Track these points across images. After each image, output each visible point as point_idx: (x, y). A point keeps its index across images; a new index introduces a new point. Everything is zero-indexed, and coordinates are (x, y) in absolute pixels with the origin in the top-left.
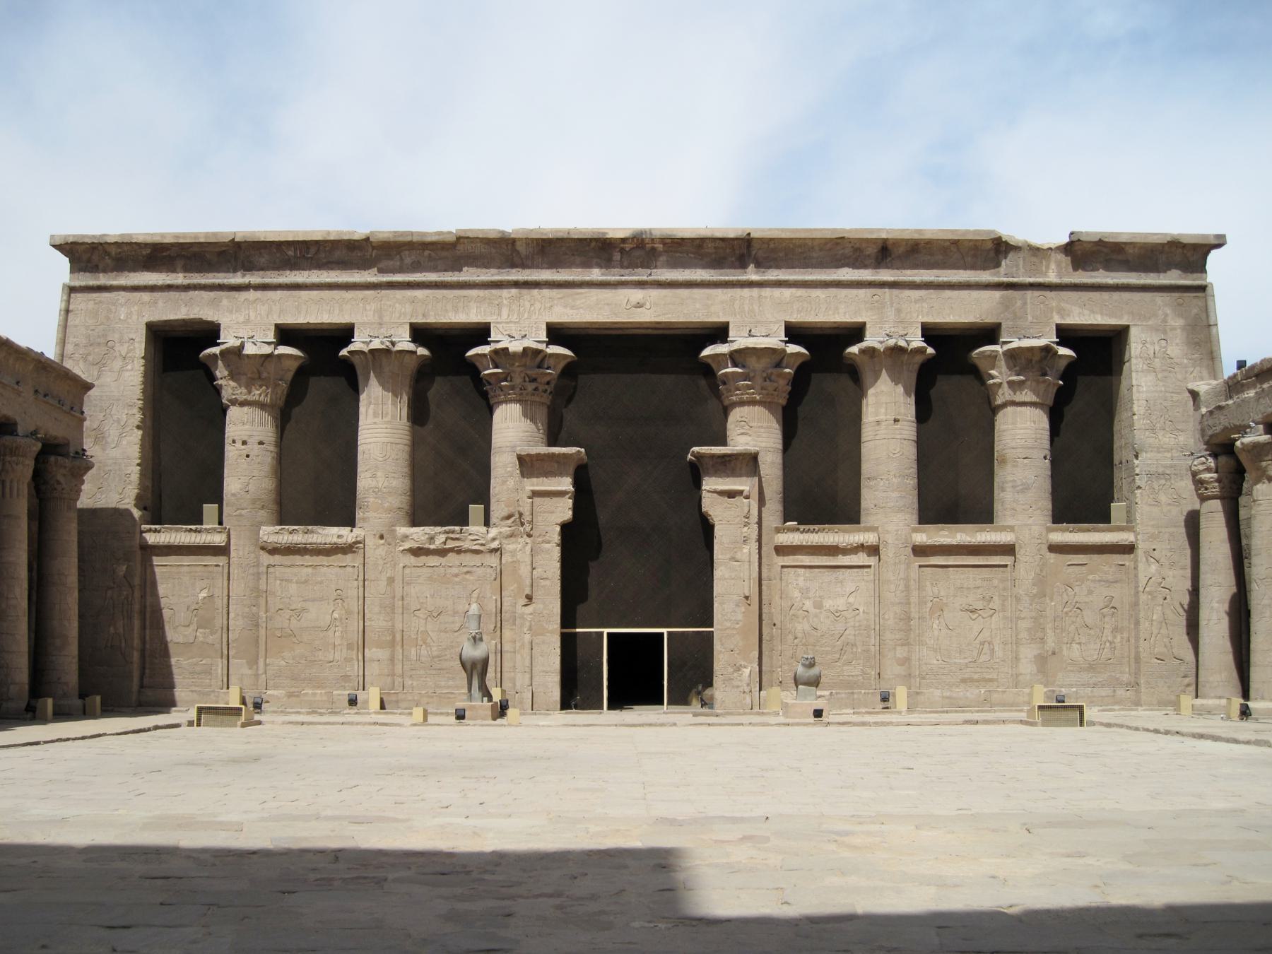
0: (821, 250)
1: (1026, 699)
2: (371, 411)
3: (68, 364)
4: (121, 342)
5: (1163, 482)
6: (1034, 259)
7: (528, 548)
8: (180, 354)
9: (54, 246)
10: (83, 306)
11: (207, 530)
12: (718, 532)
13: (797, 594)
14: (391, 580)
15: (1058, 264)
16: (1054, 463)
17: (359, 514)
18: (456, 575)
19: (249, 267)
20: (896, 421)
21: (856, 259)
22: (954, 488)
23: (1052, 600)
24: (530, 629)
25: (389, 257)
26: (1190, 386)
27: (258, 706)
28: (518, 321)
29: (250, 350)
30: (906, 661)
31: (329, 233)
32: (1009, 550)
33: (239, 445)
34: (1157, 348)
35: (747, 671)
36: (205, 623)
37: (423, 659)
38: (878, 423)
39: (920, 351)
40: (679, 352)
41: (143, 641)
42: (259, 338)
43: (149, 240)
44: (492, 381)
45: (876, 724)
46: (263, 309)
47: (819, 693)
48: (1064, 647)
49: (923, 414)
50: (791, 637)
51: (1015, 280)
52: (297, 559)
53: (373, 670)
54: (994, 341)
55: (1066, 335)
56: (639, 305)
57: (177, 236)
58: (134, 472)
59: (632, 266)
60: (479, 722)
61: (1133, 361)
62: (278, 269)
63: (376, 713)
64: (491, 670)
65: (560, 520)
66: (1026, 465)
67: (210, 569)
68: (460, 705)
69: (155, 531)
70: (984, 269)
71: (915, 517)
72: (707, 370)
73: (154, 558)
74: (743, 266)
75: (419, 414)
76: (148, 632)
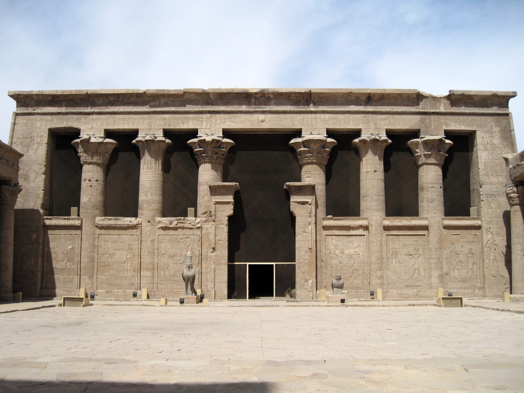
0: (342, 98)
1: (435, 294)
2: (145, 167)
3: (14, 147)
4: (37, 137)
5: (493, 198)
6: (434, 102)
7: (214, 227)
8: (63, 142)
9: (10, 96)
10: (21, 121)
11: (72, 219)
12: (298, 219)
14: (153, 241)
15: (445, 104)
16: (444, 190)
17: (140, 212)
18: (182, 239)
19: (93, 105)
20: (375, 171)
21: (357, 102)
22: (401, 201)
23: (445, 250)
24: (214, 263)
25: (154, 100)
26: (504, 156)
27: (92, 297)
28: (210, 128)
29: (93, 140)
30: (381, 277)
31: (128, 90)
32: (425, 228)
33: (87, 181)
34: (488, 140)
35: (311, 282)
38: (367, 172)
40: (281, 141)
41: (43, 267)
43: (51, 93)
44: (199, 154)
45: (369, 306)
46: (99, 123)
47: (343, 291)
48: (451, 271)
49: (387, 168)
50: (330, 266)
51: (426, 111)
52: (112, 232)
53: (144, 281)
54: (417, 137)
55: (449, 134)
56: (263, 121)
57: (63, 92)
58: (41, 193)
59: (260, 104)
60: (190, 305)
61: (478, 146)
62: (106, 105)
63: (145, 300)
64: (196, 283)
65: (228, 215)
66: (432, 191)
67: (73, 236)
68: (182, 297)
69: (50, 219)
70: (413, 106)
71: (384, 213)
72: (292, 149)
73: (49, 231)
74: (308, 104)
75: (166, 168)
76: (45, 264)
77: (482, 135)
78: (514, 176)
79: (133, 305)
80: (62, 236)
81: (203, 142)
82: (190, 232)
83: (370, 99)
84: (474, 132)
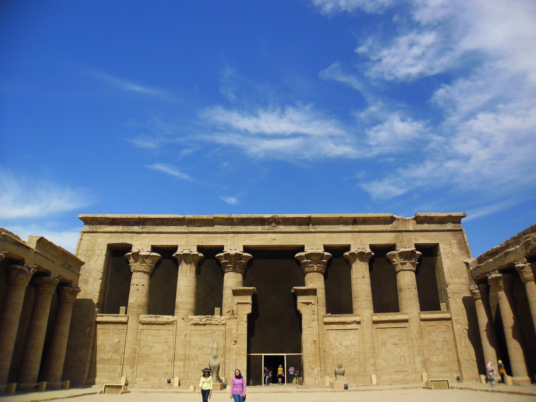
4: (98, 250)
8: (118, 255)
12: (304, 317)
13: (333, 340)
14: (186, 335)
15: (413, 224)
17: (176, 311)
18: (209, 333)
22: (385, 299)
24: (236, 354)
28: (234, 244)
29: (142, 253)
30: (374, 365)
32: (406, 321)
33: (135, 286)
35: (316, 370)
36: (116, 351)
37: (196, 366)
39: (370, 253)
42: (145, 250)
44: (224, 265)
52: (153, 327)
53: (177, 370)
56: (274, 239)
64: (220, 372)
65: (247, 313)
69: (102, 316)
77: (444, 246)
78: (475, 276)
79: (166, 392)
80: (111, 330)
81: (228, 256)
82: (216, 328)
83: (355, 221)
84: (438, 244)
